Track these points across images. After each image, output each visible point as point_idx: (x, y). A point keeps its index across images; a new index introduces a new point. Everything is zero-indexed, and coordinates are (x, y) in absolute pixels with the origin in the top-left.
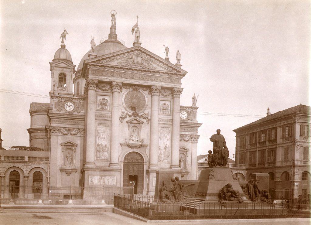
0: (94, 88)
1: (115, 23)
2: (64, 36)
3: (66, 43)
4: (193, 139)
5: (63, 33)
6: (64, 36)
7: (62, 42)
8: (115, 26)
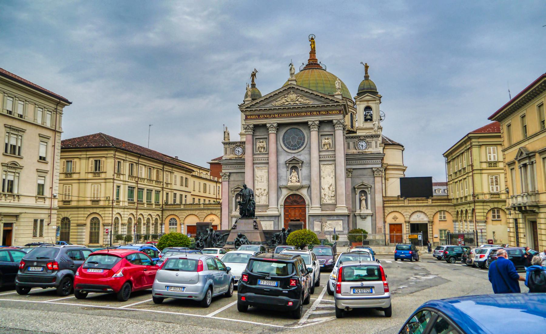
0: (249, 133)
1: (314, 47)
2: (253, 75)
3: (256, 81)
4: (375, 173)
5: (253, 72)
6: (253, 75)
7: (253, 81)
8: (315, 50)
